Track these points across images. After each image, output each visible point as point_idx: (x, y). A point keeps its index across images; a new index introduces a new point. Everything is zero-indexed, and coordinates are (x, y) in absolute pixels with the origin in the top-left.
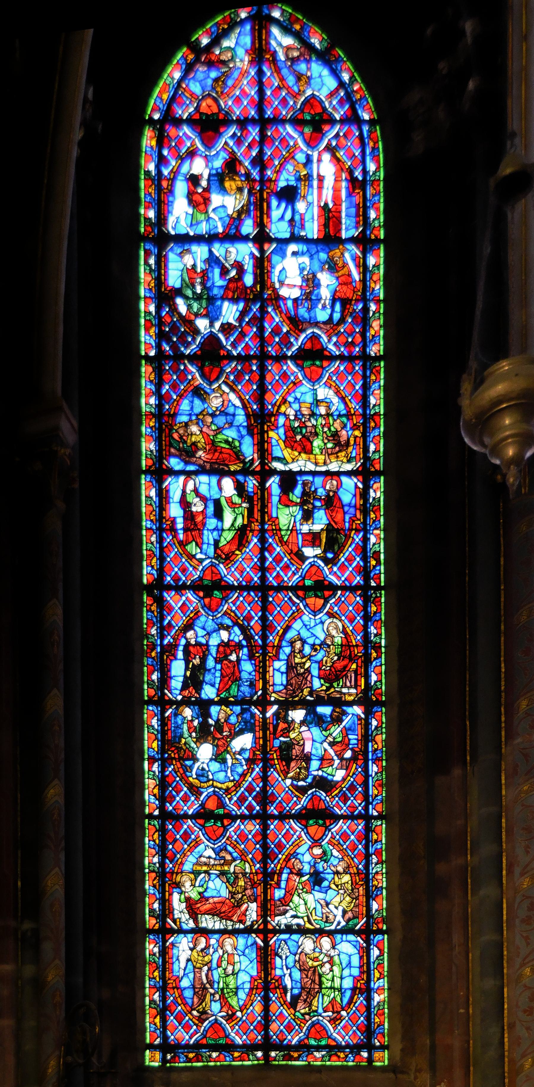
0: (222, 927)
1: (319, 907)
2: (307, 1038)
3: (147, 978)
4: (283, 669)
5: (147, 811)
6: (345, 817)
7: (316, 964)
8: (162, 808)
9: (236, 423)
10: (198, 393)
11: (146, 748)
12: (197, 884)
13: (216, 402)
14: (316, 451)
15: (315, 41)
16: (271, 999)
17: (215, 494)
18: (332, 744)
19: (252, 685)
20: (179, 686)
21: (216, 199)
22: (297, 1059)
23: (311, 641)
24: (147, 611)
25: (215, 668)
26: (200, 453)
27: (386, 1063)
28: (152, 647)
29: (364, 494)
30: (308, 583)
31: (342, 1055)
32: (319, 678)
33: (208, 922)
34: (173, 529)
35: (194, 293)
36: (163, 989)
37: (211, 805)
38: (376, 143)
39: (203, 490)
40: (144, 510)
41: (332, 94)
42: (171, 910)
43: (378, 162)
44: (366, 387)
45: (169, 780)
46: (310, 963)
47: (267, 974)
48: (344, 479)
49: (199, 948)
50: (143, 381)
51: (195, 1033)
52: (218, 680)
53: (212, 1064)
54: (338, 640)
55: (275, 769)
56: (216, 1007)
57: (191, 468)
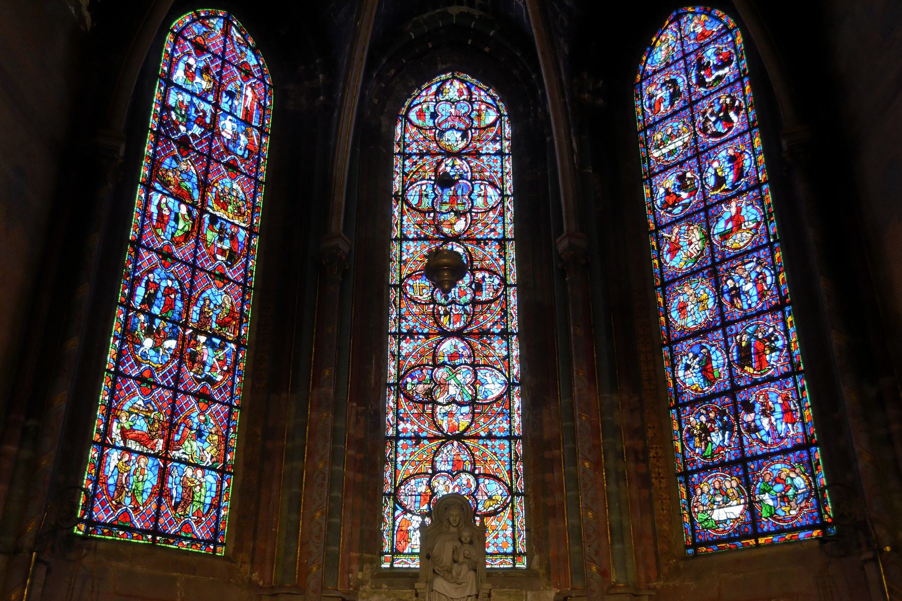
0: (140, 450)
1: (198, 451)
2: (180, 531)
3: (86, 473)
4: (198, 312)
5: (107, 367)
6: (220, 403)
7: (192, 485)
8: (116, 367)
9: (192, 181)
10: (175, 158)
11: (114, 330)
12: (130, 420)
13: (184, 167)
14: (229, 211)
16: (162, 502)
17: (176, 209)
18: (218, 360)
19: (180, 314)
20: (140, 301)
21: (198, 79)
22: (172, 544)
23: (214, 302)
24: (129, 254)
25: (161, 298)
26: (171, 187)
27: (223, 555)
28: (128, 275)
29: (249, 240)
30: (217, 272)
31: (199, 546)
32: (216, 323)
33: (132, 445)
34: (151, 217)
35: (181, 113)
36: (96, 482)
37: (146, 374)
38: (271, 94)
39: (170, 205)
40: (136, 202)
41: (254, 66)
42: (111, 432)
43: (271, 102)
44: (255, 192)
45: (124, 352)
47: (163, 486)
48: (241, 230)
49: (124, 460)
51: (112, 515)
52: (162, 306)
53: (118, 539)
54: (228, 306)
55: (186, 365)
56: (128, 501)
57: (166, 192)
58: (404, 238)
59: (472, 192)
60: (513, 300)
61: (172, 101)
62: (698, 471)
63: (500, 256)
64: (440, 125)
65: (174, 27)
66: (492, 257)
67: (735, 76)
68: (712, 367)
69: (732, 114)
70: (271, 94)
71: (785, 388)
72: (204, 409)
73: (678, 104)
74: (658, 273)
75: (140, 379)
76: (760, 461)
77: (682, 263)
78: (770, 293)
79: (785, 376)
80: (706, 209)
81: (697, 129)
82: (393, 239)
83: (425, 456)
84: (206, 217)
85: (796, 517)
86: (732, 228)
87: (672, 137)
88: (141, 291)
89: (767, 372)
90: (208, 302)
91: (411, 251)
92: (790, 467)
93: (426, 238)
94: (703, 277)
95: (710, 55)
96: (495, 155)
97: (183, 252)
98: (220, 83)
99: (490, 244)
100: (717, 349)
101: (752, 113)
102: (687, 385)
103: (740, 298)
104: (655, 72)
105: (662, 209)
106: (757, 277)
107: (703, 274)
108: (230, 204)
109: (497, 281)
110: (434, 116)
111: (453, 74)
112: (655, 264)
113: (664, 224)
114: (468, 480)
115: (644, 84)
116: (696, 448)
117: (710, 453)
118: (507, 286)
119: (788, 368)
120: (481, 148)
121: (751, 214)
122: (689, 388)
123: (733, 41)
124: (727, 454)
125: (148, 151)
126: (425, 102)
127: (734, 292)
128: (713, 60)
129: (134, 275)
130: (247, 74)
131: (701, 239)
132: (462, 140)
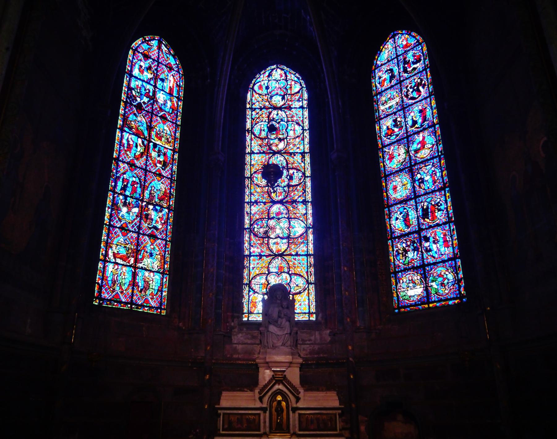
0: (123, 263)
1: (151, 263)
2: (144, 303)
3: (98, 275)
4: (149, 193)
5: (105, 222)
6: (161, 239)
7: (148, 280)
8: (110, 222)
10: (135, 114)
12: (117, 248)
13: (139, 119)
14: (163, 141)
15: (172, 52)
18: (159, 218)
19: (140, 195)
20: (120, 189)
21: (145, 73)
22: (140, 309)
23: (156, 188)
26: (133, 130)
28: (114, 175)
29: (173, 155)
30: (157, 173)
31: (153, 310)
32: (158, 198)
33: (119, 261)
34: (123, 146)
36: (102, 279)
37: (124, 226)
38: (183, 79)
39: (133, 139)
42: (108, 255)
43: (183, 83)
44: (176, 130)
46: (147, 280)
48: (168, 150)
49: (115, 268)
50: (121, 106)
52: (131, 191)
53: (114, 307)
54: (164, 190)
56: (117, 288)
58: (252, 153)
59: (287, 128)
60: (309, 184)
61: (133, 85)
62: (401, 271)
63: (302, 161)
64: (270, 93)
65: (134, 47)
66: (298, 162)
67: (422, 68)
68: (409, 219)
69: (421, 88)
70: (183, 79)
71: (445, 230)
72: (153, 242)
73: (394, 82)
74: (383, 170)
75: (121, 228)
76: (432, 266)
77: (395, 165)
78: (438, 181)
79: (445, 223)
80: (407, 137)
81: (403, 95)
82: (246, 153)
83: (264, 265)
84: (151, 144)
85: (448, 294)
86: (420, 147)
87: (390, 99)
88: (120, 184)
89: (435, 222)
90: (153, 188)
91: (256, 159)
92: (446, 269)
93: (264, 152)
94: (406, 173)
95: (410, 57)
96: (300, 108)
97: (140, 163)
98: (157, 74)
99: (297, 155)
100: (412, 210)
101: (431, 87)
102: (397, 228)
103: (424, 184)
104: (382, 65)
105: (385, 137)
106: (432, 173)
107: (406, 171)
108: (163, 137)
109: (300, 175)
110: (267, 88)
111: (277, 66)
112: (381, 165)
113: (386, 144)
114: (286, 277)
115: (376, 71)
116: (400, 259)
117: (407, 262)
118: (305, 177)
119: (446, 220)
120: (292, 105)
121: (430, 140)
122: (397, 229)
123: (422, 49)
124: (416, 263)
125: (121, 112)
126: (263, 80)
127: (420, 181)
128: (412, 59)
129: (116, 176)
130: (171, 69)
131: (405, 153)
132: (282, 100)
